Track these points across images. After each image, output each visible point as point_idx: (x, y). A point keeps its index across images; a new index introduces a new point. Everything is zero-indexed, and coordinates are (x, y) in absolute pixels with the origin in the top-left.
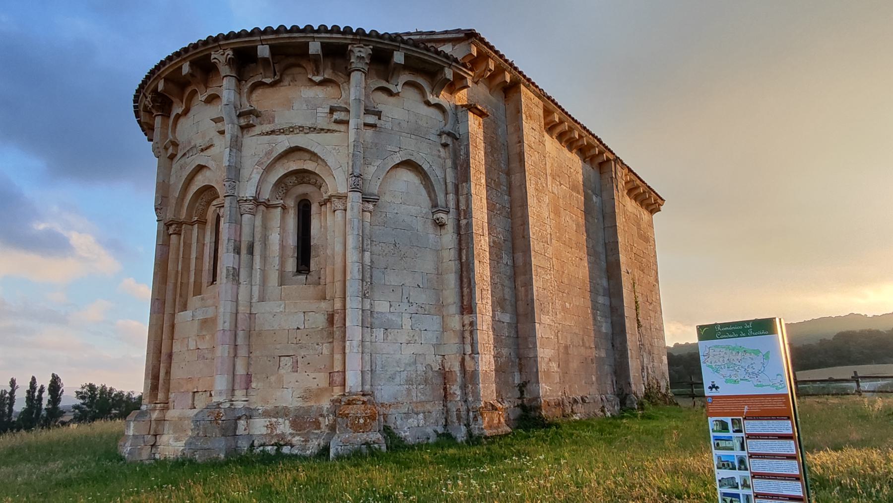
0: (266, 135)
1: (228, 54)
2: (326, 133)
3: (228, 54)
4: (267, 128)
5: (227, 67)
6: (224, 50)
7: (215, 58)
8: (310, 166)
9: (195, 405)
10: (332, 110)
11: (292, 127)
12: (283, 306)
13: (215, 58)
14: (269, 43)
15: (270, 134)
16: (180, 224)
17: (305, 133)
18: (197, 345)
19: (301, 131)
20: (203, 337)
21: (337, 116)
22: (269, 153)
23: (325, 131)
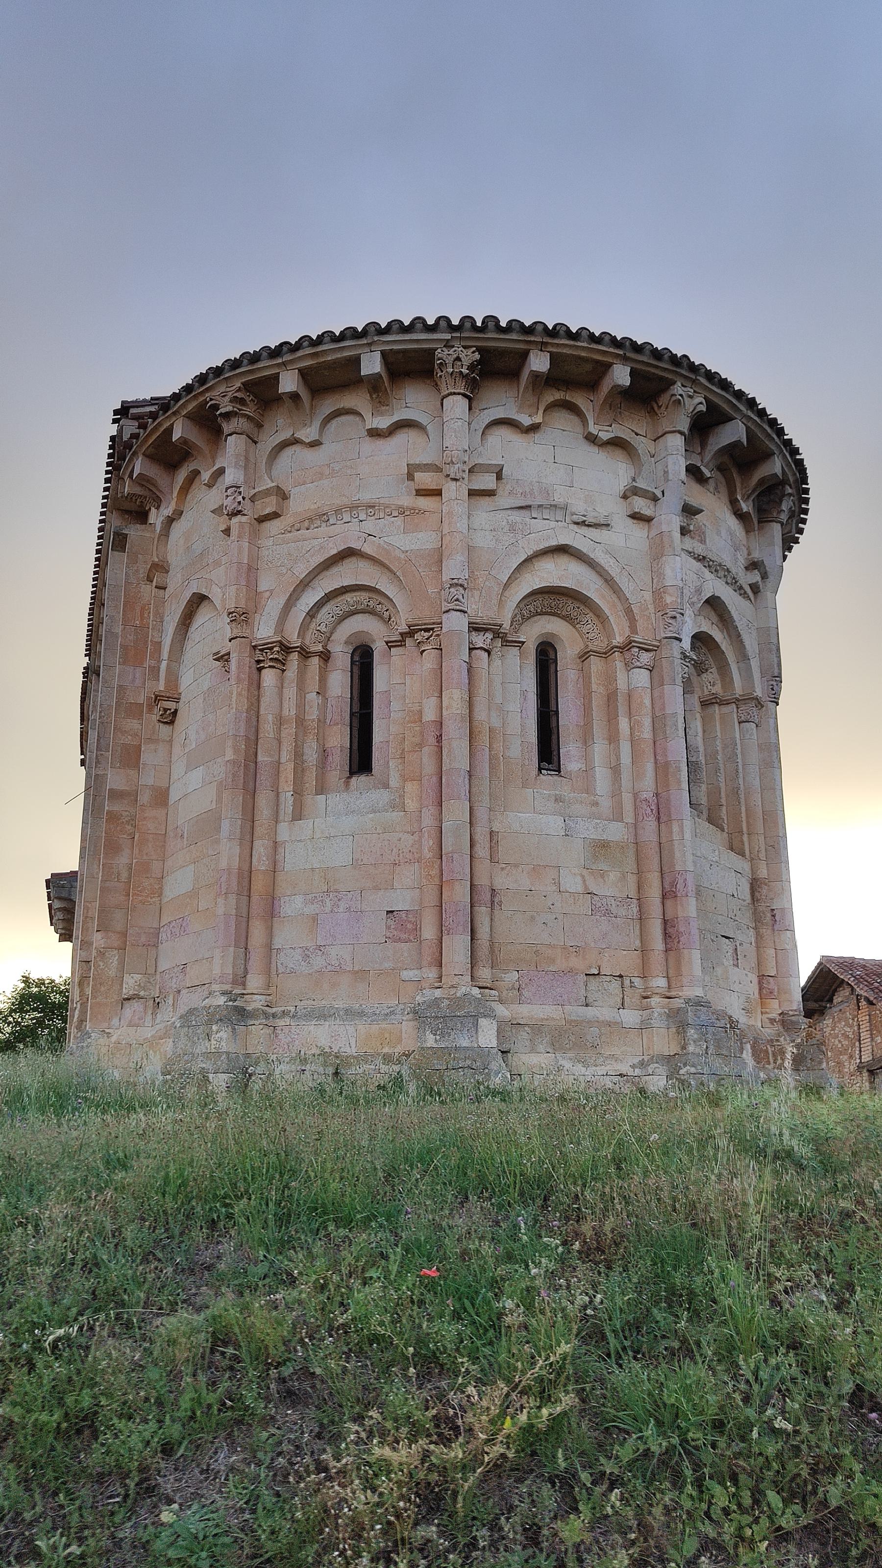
0: (695, 558)
1: (701, 403)
2: (741, 595)
3: (701, 403)
4: (700, 549)
5: (689, 420)
6: (695, 392)
7: (681, 395)
8: (718, 635)
9: (590, 1000)
10: (754, 565)
11: (720, 565)
12: (717, 853)
13: (681, 395)
14: (749, 424)
15: (700, 560)
16: (497, 633)
17: (727, 583)
18: (586, 887)
19: (725, 576)
20: (603, 874)
21: (755, 577)
22: (699, 591)
23: (742, 592)
